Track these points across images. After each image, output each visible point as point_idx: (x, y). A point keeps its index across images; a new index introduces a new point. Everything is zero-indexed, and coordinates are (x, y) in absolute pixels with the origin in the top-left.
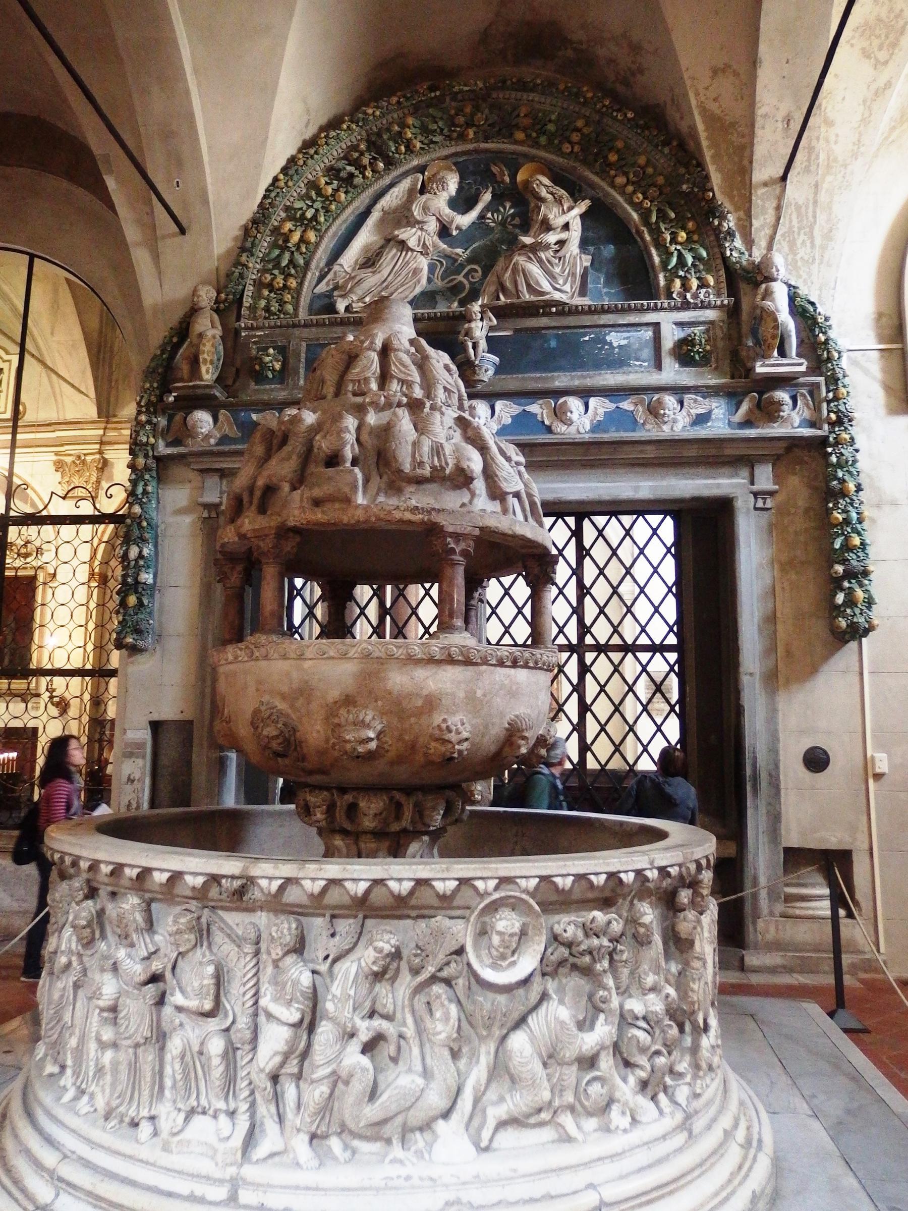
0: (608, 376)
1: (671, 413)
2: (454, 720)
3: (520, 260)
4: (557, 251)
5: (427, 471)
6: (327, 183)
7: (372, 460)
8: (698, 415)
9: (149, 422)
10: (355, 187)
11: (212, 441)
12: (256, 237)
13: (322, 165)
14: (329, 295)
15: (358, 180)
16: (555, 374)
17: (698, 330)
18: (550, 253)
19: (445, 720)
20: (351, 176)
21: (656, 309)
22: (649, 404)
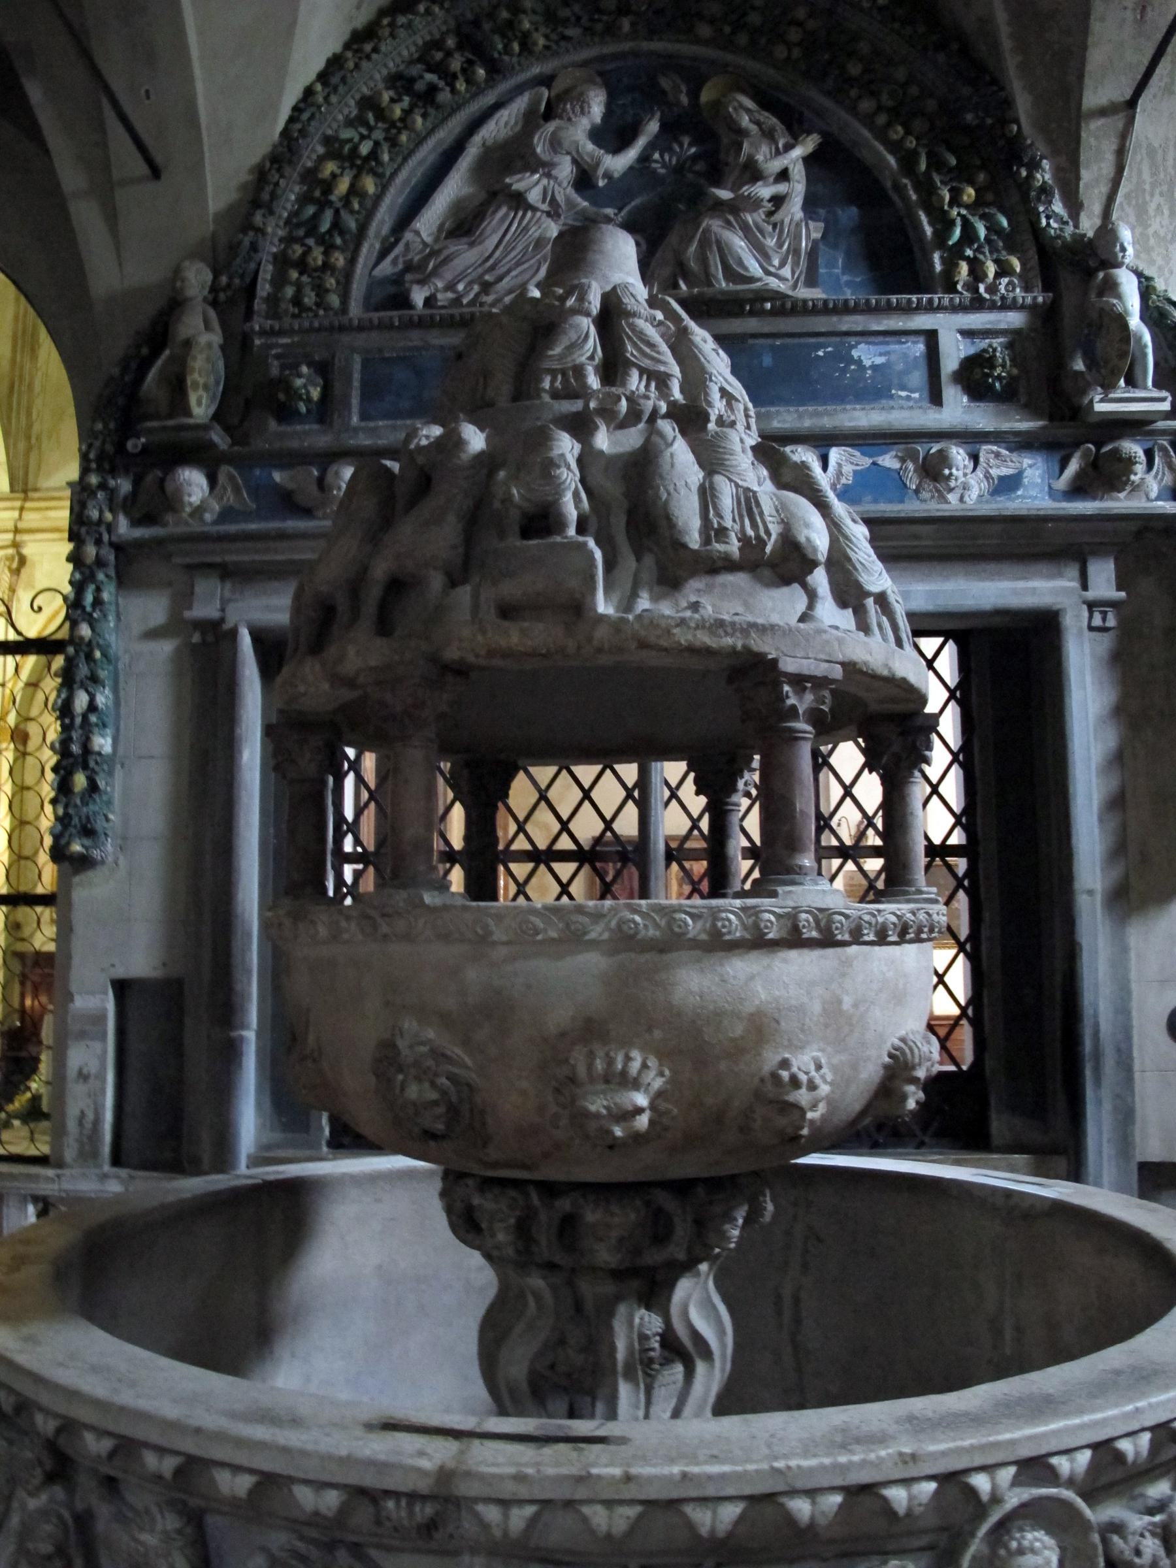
0: (857, 414)
1: (960, 474)
2: (802, 1062)
3: (715, 225)
4: (770, 214)
5: (733, 547)
6: (392, 100)
7: (619, 523)
8: (1001, 478)
9: (103, 486)
10: (438, 107)
11: (208, 517)
12: (277, 184)
13: (385, 72)
14: (397, 280)
15: (444, 96)
16: (773, 409)
17: (997, 342)
18: (760, 215)
19: (785, 1064)
20: (432, 89)
21: (930, 308)
22: (925, 458)
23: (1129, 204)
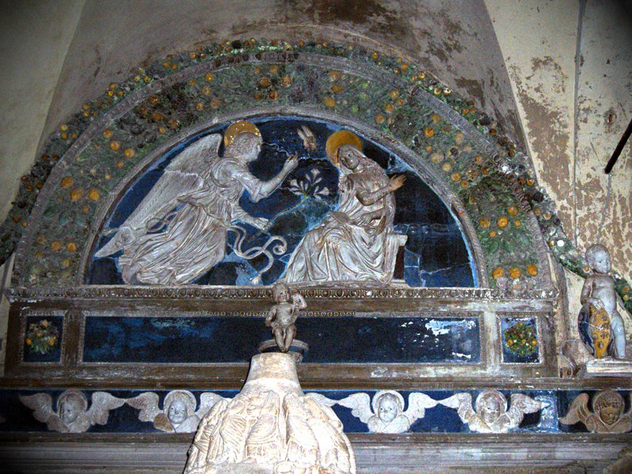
0: (429, 369)
23: (609, 232)
